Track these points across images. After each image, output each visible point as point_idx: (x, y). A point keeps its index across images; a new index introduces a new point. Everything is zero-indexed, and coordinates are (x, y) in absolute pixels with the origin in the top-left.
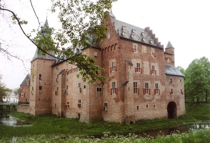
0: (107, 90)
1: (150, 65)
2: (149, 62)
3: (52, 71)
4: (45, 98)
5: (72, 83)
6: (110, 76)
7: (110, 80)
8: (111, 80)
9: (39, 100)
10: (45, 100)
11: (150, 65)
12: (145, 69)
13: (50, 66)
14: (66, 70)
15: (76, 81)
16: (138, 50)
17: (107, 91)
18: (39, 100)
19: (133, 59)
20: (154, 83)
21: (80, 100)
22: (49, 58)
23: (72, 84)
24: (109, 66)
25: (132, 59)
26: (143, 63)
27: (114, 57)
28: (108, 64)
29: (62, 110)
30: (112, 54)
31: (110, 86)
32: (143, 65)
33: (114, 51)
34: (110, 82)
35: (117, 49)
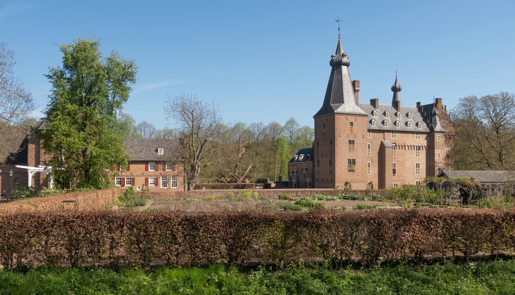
23: (405, 163)
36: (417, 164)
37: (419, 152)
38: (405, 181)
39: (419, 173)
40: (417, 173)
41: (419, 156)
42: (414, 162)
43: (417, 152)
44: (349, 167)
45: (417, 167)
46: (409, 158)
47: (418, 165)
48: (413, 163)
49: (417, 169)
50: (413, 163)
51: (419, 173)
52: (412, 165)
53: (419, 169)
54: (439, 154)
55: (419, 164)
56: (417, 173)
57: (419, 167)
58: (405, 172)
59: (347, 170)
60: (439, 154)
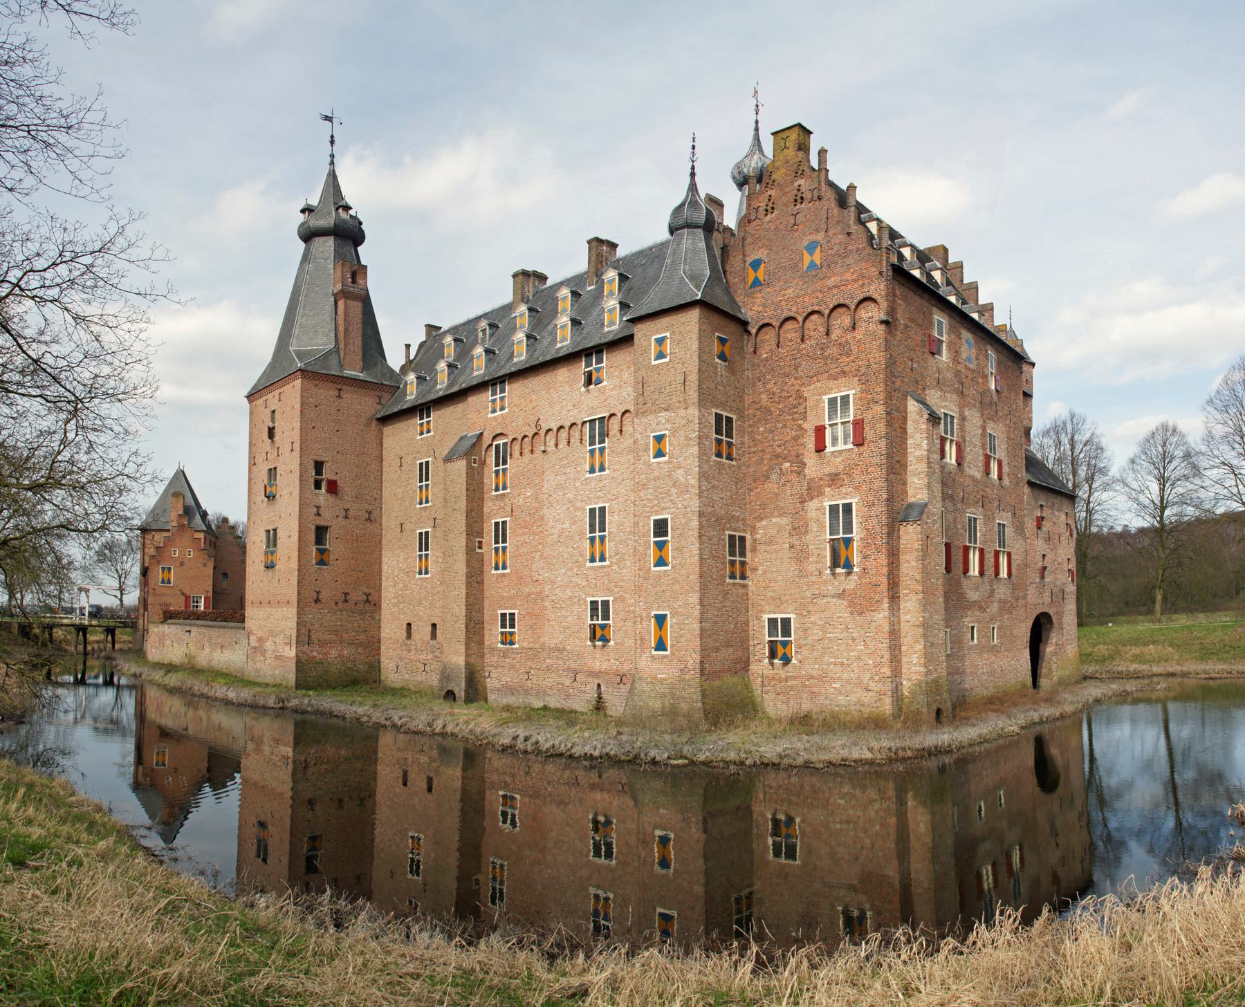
0: (791, 547)
1: (984, 429)
2: (982, 415)
3: (381, 444)
4: (346, 594)
5: (538, 510)
6: (814, 467)
7: (813, 491)
8: (820, 494)
9: (317, 601)
10: (346, 601)
11: (984, 429)
12: (968, 450)
13: (370, 420)
14: (487, 440)
15: (570, 496)
16: (949, 349)
17: (786, 554)
18: (317, 601)
19: (932, 392)
20: (994, 519)
21: (606, 603)
22: (362, 376)
23: (542, 518)
24: (805, 418)
25: (927, 392)
26: (963, 419)
27: (844, 373)
28: (801, 409)
29: (467, 656)
30: (829, 351)
31: (813, 527)
32: (962, 428)
33: (849, 336)
34: (812, 505)
35: (873, 327)
36: (592, 511)
37: (602, 450)
38: (542, 599)
39: (602, 559)
40: (593, 560)
41: (602, 469)
42: (579, 504)
43: (592, 452)
44: (325, 560)
45: (592, 530)
46: (560, 486)
47: (598, 519)
48: (576, 509)
49: (592, 540)
50: (576, 509)
51: (602, 559)
52: (573, 523)
53: (602, 539)
54: (659, 439)
55: (602, 510)
56: (593, 560)
57: (602, 529)
58: (541, 557)
59: (262, 568)
60: (659, 439)
